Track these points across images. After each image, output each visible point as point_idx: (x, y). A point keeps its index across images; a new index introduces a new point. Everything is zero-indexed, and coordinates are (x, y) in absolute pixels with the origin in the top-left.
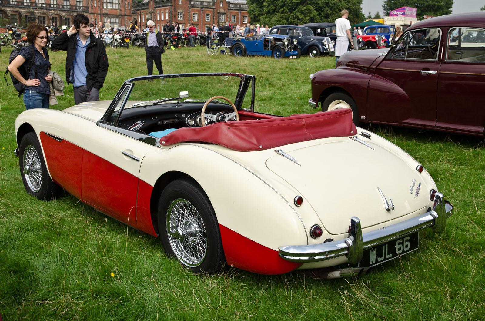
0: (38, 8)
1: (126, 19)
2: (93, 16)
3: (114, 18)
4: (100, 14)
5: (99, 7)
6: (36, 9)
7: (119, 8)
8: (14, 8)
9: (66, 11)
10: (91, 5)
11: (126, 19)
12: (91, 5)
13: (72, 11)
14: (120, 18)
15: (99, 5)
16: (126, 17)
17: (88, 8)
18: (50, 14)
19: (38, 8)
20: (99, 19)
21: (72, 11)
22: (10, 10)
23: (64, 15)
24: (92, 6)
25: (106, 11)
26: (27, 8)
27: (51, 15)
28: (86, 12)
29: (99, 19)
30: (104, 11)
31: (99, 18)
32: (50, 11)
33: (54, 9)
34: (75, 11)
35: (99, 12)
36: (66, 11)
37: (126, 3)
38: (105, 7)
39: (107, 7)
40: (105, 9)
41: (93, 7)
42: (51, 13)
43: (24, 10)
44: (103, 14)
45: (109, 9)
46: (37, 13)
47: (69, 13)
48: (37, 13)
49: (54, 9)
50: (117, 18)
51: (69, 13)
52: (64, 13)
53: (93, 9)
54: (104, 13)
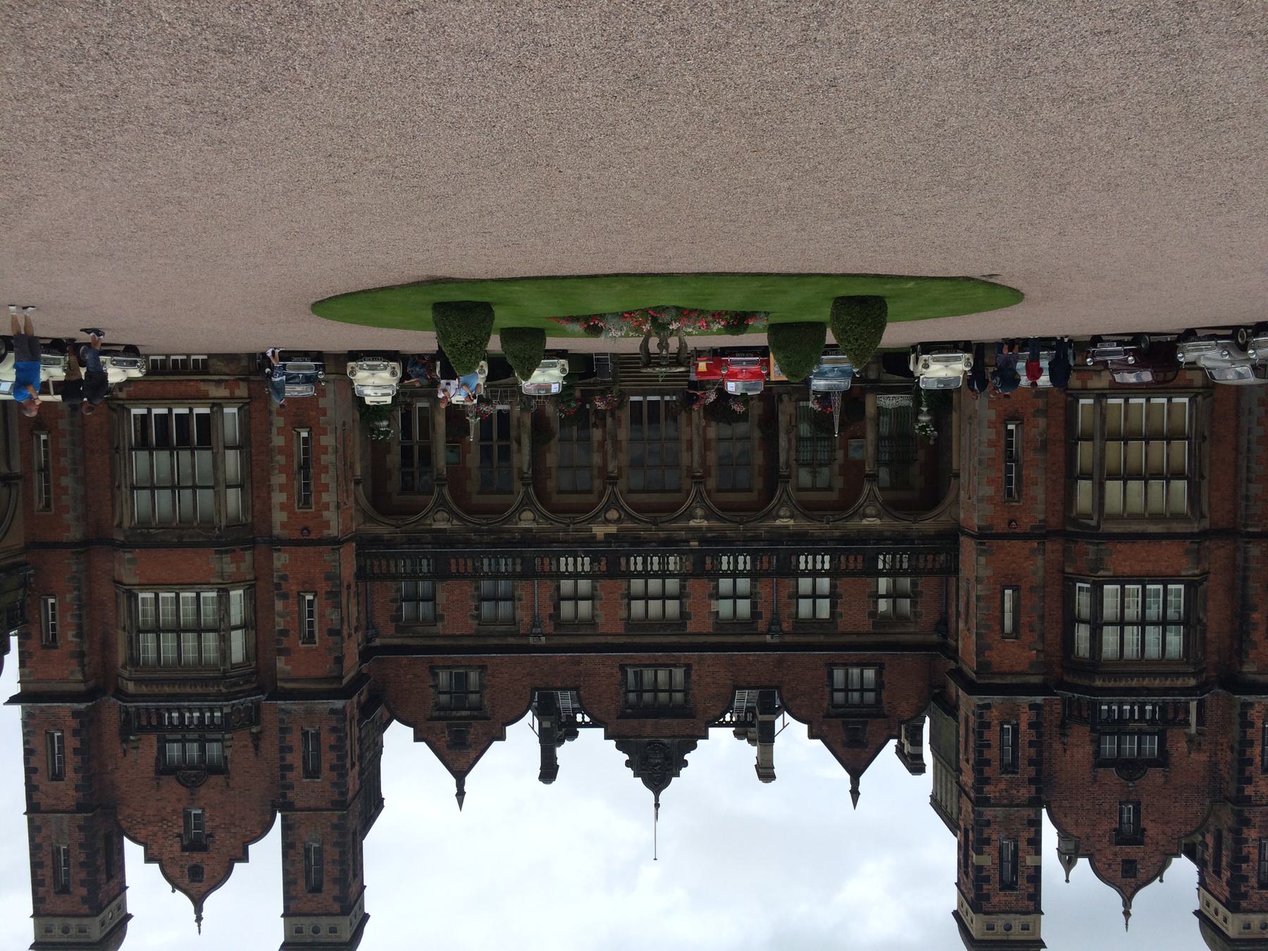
0: (694, 544)
1: (69, 517)
2: (327, 525)
3: (165, 525)
4: (278, 543)
5: (284, 596)
6: (703, 541)
7: (132, 597)
8: (837, 533)
9: (511, 543)
10: (338, 606)
11: (69, 517)
12: (338, 606)
13: (468, 543)
14: (120, 525)
15: (279, 605)
16: (75, 534)
17: (361, 575)
18: (613, 514)
19: (694, 544)
20: (283, 507)
21: (468, 543)
22: (865, 516)
23: (528, 515)
24: (334, 595)
25: (230, 568)
26: (756, 539)
27: (606, 509)
28: (376, 540)
29: (283, 507)
30: (245, 563)
31: (279, 517)
32: (613, 529)
33: (587, 544)
34: (451, 543)
35: (281, 559)
36: (511, 543)
37: (70, 635)
38: (236, 595)
39: (223, 601)
40: (236, 584)
41: (324, 587)
42: (607, 522)
43: (778, 522)
44: (252, 544)
45: (209, 585)
46: (699, 512)
47: (490, 532)
48: (699, 512)
49: (587, 544)
50: (144, 524)
51: (490, 532)
52: (523, 525)
53: (328, 578)
54: (248, 556)
